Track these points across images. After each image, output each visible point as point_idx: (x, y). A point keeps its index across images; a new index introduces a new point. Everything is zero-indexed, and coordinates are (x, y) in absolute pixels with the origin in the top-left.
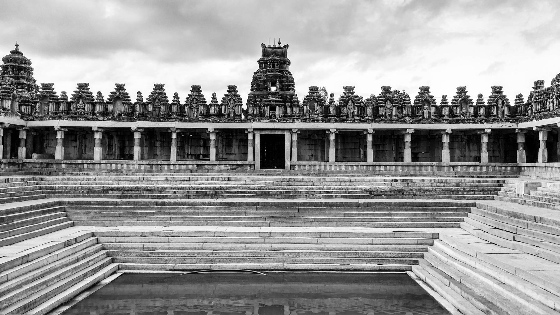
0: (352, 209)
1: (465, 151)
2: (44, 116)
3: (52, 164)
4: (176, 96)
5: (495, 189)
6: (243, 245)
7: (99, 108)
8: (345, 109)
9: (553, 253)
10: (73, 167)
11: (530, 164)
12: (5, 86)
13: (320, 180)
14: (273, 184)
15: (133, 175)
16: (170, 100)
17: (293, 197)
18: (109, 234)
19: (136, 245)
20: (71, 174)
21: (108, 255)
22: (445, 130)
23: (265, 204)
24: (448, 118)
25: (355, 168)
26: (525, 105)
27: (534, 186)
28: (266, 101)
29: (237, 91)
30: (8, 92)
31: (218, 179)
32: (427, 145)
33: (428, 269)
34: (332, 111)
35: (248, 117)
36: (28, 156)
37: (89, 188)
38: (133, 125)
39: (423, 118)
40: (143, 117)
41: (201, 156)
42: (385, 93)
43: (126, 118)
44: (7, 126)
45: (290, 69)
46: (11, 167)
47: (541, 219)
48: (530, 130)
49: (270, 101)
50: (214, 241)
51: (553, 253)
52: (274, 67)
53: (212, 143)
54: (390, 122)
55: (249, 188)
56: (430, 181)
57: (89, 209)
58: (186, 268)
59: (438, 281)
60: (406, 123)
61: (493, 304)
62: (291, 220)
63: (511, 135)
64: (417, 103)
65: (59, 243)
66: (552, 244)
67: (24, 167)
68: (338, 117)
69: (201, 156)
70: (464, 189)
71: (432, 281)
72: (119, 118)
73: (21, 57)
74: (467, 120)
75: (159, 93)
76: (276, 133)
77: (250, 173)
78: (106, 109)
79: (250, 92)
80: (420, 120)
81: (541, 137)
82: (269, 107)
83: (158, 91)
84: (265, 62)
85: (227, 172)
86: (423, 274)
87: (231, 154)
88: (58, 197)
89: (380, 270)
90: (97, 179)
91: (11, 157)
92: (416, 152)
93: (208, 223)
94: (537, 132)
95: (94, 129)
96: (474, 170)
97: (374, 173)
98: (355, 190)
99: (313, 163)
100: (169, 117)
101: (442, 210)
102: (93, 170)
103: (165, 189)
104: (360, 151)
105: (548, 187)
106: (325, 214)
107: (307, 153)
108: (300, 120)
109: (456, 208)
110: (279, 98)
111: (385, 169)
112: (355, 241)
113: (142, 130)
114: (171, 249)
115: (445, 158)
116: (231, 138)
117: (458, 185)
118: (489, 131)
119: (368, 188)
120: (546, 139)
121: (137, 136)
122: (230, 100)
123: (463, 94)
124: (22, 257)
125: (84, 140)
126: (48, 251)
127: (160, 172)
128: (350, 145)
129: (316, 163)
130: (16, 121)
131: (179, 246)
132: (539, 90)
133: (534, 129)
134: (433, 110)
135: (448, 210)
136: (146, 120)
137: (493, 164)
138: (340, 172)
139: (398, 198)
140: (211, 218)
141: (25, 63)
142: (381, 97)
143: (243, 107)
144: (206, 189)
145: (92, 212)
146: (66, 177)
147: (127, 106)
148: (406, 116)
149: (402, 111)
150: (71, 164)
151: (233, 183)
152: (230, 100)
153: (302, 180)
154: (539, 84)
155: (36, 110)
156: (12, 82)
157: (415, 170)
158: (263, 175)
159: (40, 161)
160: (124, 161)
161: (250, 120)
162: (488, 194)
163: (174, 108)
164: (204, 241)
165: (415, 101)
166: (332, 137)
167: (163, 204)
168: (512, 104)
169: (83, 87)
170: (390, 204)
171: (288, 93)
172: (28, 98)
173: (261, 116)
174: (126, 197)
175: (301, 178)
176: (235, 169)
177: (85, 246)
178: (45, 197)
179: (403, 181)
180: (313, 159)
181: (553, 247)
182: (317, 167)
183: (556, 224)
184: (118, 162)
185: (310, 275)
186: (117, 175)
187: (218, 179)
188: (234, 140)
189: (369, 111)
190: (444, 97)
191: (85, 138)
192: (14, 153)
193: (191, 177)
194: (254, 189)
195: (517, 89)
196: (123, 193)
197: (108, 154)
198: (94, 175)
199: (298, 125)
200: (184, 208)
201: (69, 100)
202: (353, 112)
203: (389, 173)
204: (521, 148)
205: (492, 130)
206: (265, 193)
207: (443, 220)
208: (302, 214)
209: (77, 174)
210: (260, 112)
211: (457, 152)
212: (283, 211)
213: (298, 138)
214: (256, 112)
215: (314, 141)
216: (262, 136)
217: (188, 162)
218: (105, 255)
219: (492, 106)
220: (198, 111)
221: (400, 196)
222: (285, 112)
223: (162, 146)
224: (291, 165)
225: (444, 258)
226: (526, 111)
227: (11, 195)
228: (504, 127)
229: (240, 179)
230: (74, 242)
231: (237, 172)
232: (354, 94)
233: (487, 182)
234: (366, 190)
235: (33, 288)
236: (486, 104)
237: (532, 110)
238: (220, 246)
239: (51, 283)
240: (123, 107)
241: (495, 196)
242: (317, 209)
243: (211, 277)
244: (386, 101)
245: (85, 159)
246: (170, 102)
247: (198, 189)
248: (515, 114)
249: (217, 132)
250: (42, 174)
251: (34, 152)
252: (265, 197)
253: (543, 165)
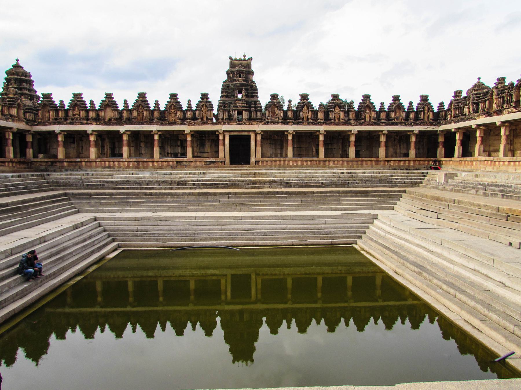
0: (308, 197)
1: (397, 148)
2: (46, 121)
3: (56, 162)
4: (157, 103)
5: (421, 179)
6: (219, 227)
7: (92, 114)
8: (301, 113)
9: (469, 227)
11: (447, 159)
12: (10, 96)
13: (280, 173)
14: (242, 177)
15: (123, 170)
16: (152, 106)
17: (258, 187)
18: (109, 219)
19: (131, 228)
20: (73, 170)
21: (109, 236)
22: (382, 131)
23: (235, 194)
24: (385, 121)
25: (309, 163)
26: (446, 111)
27: (452, 176)
28: (234, 107)
29: (209, 98)
30: (13, 101)
31: (195, 173)
32: (367, 143)
33: (370, 242)
34: (290, 115)
35: (219, 120)
36: (35, 156)
37: (89, 182)
38: (122, 128)
39: (365, 121)
40: (129, 121)
41: (179, 155)
42: (334, 100)
43: (116, 123)
44: (15, 130)
45: (255, 78)
46: (21, 165)
47: (459, 202)
48: (449, 131)
49: (237, 107)
50: (196, 224)
51: (469, 227)
52: (240, 77)
53: (189, 143)
54: (338, 124)
55: (221, 181)
56: (370, 173)
57: (90, 199)
58: (173, 245)
59: (379, 251)
60: (351, 125)
61: (424, 267)
62: (258, 207)
63: (435, 134)
64: (361, 108)
65: (67, 226)
66: (468, 221)
67: (33, 166)
68: (295, 119)
69: (179, 155)
70: (396, 179)
71: (374, 251)
72: (109, 122)
73: (22, 70)
74: (400, 123)
75: (142, 101)
76: (243, 134)
77: (221, 168)
78: (98, 115)
79: (220, 99)
80: (363, 123)
81: (457, 137)
82: (236, 111)
83: (141, 99)
84: (233, 72)
85: (202, 167)
86: (366, 245)
87: (204, 152)
88: (63, 189)
89: (332, 244)
90: (94, 175)
91: (21, 157)
92: (358, 149)
93: (189, 209)
94: (454, 133)
95: (89, 132)
96: (404, 164)
97: (324, 167)
98: (309, 181)
99: (274, 159)
100: (151, 121)
101: (380, 196)
102: (90, 167)
103: (151, 181)
104: (313, 149)
105: (462, 176)
106: (286, 201)
107: (269, 151)
108: (263, 123)
109: (391, 194)
110: (245, 104)
111: (334, 164)
112: (312, 221)
113: (129, 133)
114: (161, 230)
115: (382, 154)
116: (204, 138)
117: (392, 176)
118: (417, 132)
119: (320, 179)
120: (461, 138)
121: (125, 138)
122: (203, 106)
123: (397, 102)
124: (40, 238)
125: (80, 142)
126: (61, 233)
127: (146, 168)
128: (305, 143)
129: (277, 159)
130: (22, 126)
131: (166, 228)
132: (458, 98)
133: (453, 130)
134: (373, 114)
135: (384, 196)
136: (132, 124)
137: (419, 159)
138: (297, 166)
139: (344, 187)
140: (191, 205)
141: (26, 76)
142: (331, 103)
143: (214, 112)
144: (186, 181)
145: (93, 201)
146: (68, 173)
147: (116, 113)
148: (351, 120)
149: (348, 115)
150: (71, 162)
151: (208, 177)
152: (203, 106)
153: (266, 173)
154: (457, 94)
155: (38, 116)
156: (16, 92)
157: (358, 165)
158: (232, 170)
159: (46, 160)
160: (115, 159)
161: (221, 124)
162: (415, 183)
163: (156, 114)
164: (186, 224)
165: (359, 106)
166: (290, 138)
167: (151, 194)
168: (436, 110)
169: (78, 97)
170: (339, 192)
171: (252, 99)
172: (31, 106)
173: (230, 120)
174: (119, 189)
175: (265, 171)
176: (209, 165)
177: (90, 229)
178: (52, 190)
179: (349, 173)
180: (274, 156)
181: (469, 222)
182: (278, 163)
183: (471, 205)
184: (111, 159)
185: (275, 250)
186: (110, 171)
187: (195, 173)
188: (207, 141)
189: (321, 115)
190: (382, 104)
191: (81, 140)
192: (23, 153)
193: (172, 172)
194: (226, 181)
195: (441, 97)
196: (117, 185)
197: (101, 154)
198: (91, 171)
199: (261, 127)
200: (168, 197)
201: (67, 107)
202: (308, 116)
203: (336, 167)
204: (441, 146)
205: (419, 131)
206: (235, 185)
207: (381, 204)
208: (267, 201)
209: (77, 170)
210: (229, 116)
211: (391, 150)
212: (251, 199)
213: (262, 138)
214: (226, 116)
215: (274, 141)
216: (231, 137)
217: (169, 159)
218: (107, 236)
219: (420, 111)
220: (176, 115)
221: (346, 185)
222: (250, 116)
223: (146, 147)
224: (255, 161)
225: (383, 234)
226: (446, 115)
227: (24, 188)
228: (429, 129)
229: (214, 173)
230: (80, 225)
231: (211, 167)
232: (309, 101)
233: (414, 173)
234: (318, 180)
235: (51, 262)
236: (415, 110)
237: (451, 115)
238: (201, 227)
239: (66, 258)
240: (113, 114)
241: (421, 184)
242: (279, 197)
243: (194, 253)
244: (335, 107)
245: (82, 158)
246: (152, 108)
247: (178, 182)
248: (439, 117)
249: (193, 133)
250: (48, 171)
251: (40, 153)
252: (235, 188)
253: (458, 159)
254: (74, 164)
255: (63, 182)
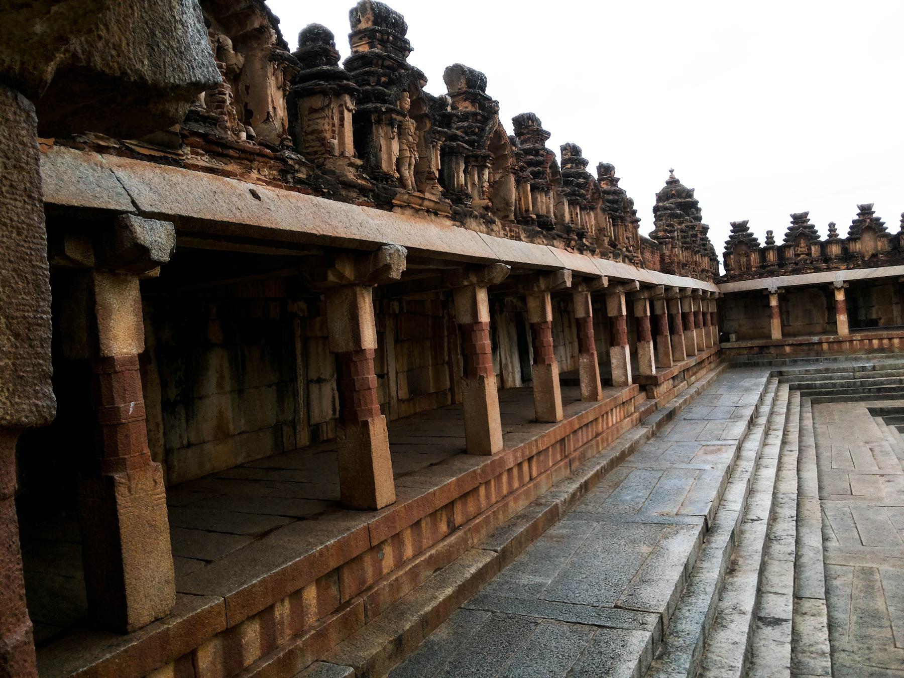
3: (768, 347)
10: (803, 350)
20: (807, 361)
37: (875, 383)
72: (874, 261)
102: (841, 352)
150: (801, 345)
169: (800, 220)
198: (847, 359)
254: (805, 348)
255: (822, 386)
